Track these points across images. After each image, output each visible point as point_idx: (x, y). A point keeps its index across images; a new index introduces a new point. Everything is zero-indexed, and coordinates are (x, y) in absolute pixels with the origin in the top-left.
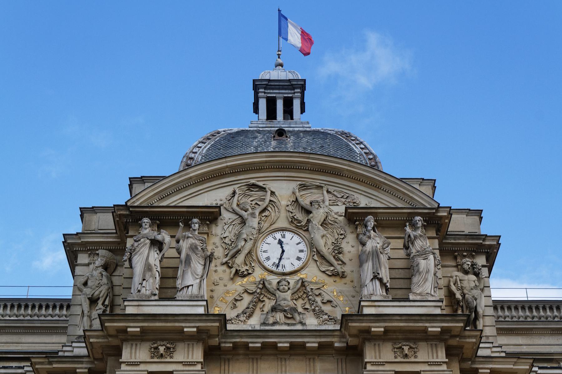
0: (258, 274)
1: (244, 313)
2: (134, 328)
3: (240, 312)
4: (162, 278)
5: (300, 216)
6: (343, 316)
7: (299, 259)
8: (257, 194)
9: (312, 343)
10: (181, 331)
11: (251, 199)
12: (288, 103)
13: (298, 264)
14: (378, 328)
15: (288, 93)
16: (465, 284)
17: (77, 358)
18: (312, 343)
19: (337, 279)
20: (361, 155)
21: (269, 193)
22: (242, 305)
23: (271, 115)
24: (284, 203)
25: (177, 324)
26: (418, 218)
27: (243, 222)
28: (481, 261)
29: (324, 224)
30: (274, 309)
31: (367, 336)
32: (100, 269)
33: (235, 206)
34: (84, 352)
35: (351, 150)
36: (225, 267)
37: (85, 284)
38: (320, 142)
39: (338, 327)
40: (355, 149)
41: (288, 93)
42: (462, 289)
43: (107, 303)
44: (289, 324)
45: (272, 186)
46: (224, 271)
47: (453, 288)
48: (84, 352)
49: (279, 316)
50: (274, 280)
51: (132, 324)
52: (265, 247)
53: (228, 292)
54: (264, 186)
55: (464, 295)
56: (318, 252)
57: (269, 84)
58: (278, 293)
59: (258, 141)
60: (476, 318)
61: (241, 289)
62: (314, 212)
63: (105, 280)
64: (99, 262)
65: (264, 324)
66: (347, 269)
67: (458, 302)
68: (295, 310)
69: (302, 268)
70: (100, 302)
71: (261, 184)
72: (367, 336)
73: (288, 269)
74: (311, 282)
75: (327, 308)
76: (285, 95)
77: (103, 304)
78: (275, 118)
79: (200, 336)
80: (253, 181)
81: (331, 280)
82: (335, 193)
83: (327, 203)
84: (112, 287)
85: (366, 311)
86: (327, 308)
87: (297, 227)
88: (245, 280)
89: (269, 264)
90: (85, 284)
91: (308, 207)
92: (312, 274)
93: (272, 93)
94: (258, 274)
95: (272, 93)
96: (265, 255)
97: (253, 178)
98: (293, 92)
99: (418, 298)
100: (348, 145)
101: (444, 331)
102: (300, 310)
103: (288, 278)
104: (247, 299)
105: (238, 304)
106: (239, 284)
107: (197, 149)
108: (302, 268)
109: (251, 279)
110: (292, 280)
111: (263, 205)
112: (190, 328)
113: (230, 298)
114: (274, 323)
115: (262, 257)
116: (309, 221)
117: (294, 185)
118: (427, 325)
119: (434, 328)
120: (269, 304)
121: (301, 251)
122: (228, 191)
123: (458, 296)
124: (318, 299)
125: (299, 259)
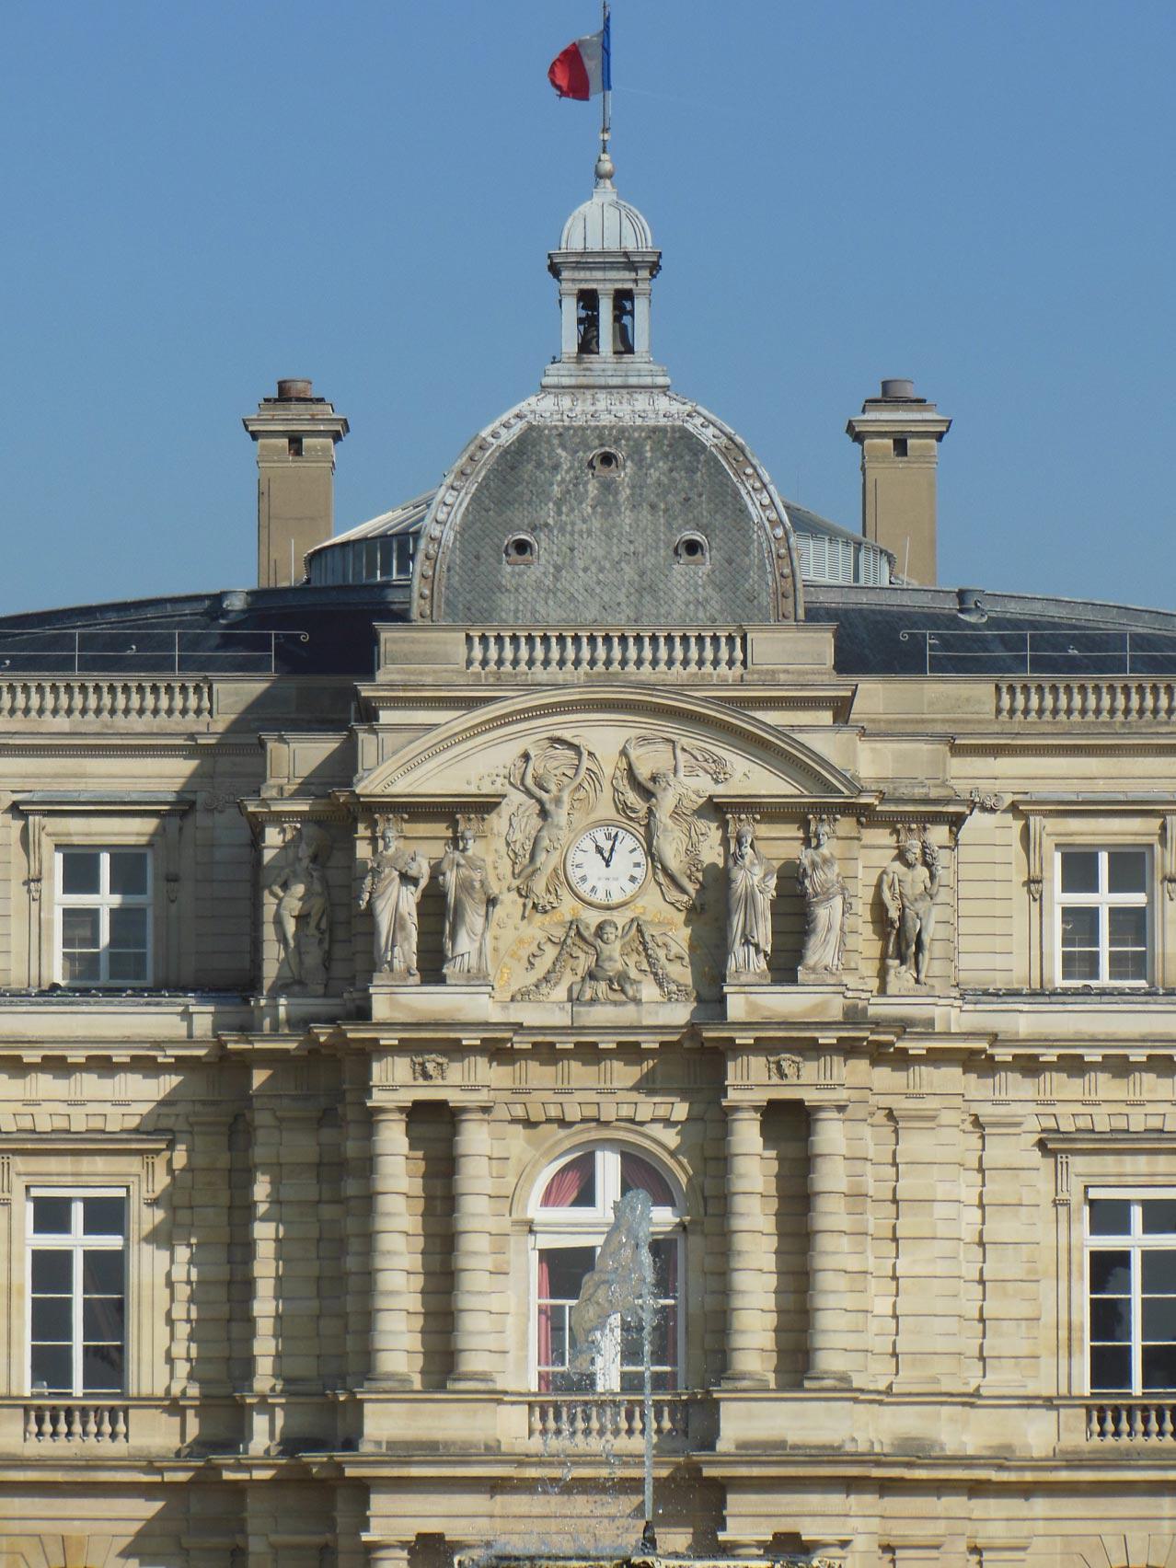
0: (568, 907)
1: (546, 979)
3: (541, 975)
7: (633, 879)
11: (556, 764)
12: (623, 299)
13: (631, 889)
15: (622, 279)
16: (908, 891)
20: (762, 527)
22: (544, 964)
25: (452, 1035)
30: (591, 976)
33: (529, 781)
35: (743, 510)
36: (514, 895)
40: (751, 509)
41: (622, 279)
43: (323, 925)
44: (615, 1003)
46: (514, 902)
50: (592, 918)
51: (386, 1035)
53: (521, 941)
54: (576, 741)
56: (665, 870)
57: (584, 261)
59: (563, 480)
61: (541, 936)
65: (574, 1000)
68: (623, 978)
70: (313, 923)
71: (567, 735)
73: (616, 898)
74: (651, 922)
76: (619, 286)
77: (318, 927)
80: (558, 734)
82: (696, 753)
87: (631, 819)
88: (547, 918)
89: (583, 889)
91: (650, 785)
94: (568, 907)
96: (579, 872)
98: (633, 275)
100: (737, 494)
102: (633, 974)
104: (551, 952)
105: (536, 961)
106: (536, 929)
107: (445, 509)
109: (555, 916)
110: (621, 918)
113: (524, 953)
114: (593, 1001)
115: (574, 875)
116: (650, 812)
118: (817, 1034)
120: (585, 962)
121: (637, 865)
125: (633, 879)
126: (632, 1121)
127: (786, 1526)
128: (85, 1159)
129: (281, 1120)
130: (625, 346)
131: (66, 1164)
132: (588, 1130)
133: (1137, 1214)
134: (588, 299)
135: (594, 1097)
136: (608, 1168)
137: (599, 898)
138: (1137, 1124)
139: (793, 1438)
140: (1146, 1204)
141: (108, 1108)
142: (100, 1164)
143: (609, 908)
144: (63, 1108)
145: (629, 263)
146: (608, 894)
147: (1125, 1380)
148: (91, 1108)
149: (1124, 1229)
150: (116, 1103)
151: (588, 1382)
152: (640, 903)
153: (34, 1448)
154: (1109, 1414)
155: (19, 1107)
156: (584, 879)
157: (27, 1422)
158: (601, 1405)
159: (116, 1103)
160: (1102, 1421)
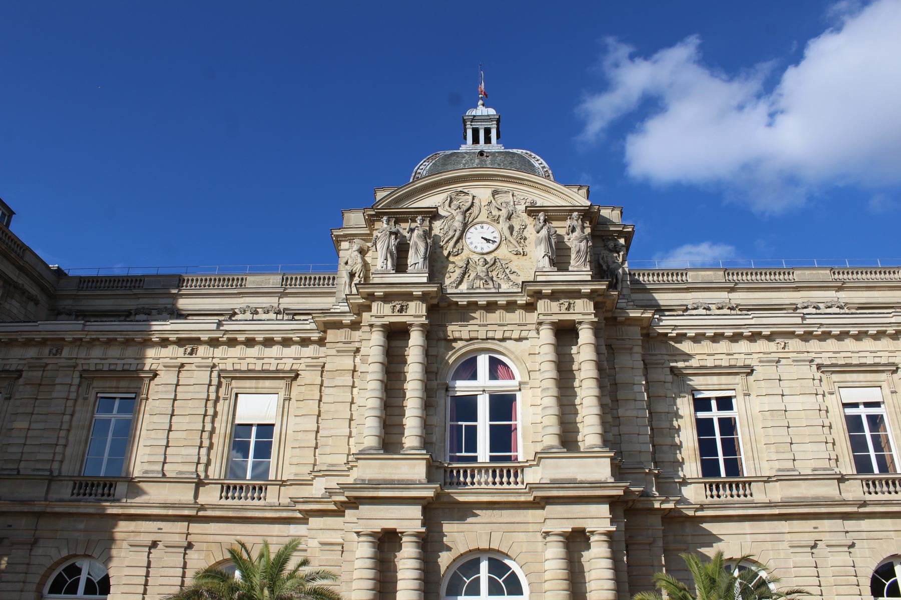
2: (379, 292)
4: (398, 258)
5: (495, 212)
6: (523, 282)
8: (463, 198)
9: (502, 301)
10: (411, 294)
12: (488, 131)
14: (547, 290)
15: (487, 125)
17: (342, 313)
18: (502, 301)
19: (520, 256)
21: (470, 198)
23: (476, 140)
24: (483, 204)
26: (576, 214)
27: (453, 218)
28: (622, 241)
29: (509, 218)
31: (538, 295)
32: (356, 253)
34: (347, 309)
37: (346, 263)
38: (509, 159)
39: (520, 290)
41: (487, 125)
42: (607, 262)
45: (473, 192)
47: (601, 262)
48: (347, 309)
49: (478, 283)
50: (475, 257)
52: (469, 235)
55: (608, 266)
57: (474, 119)
58: (479, 268)
60: (617, 282)
62: (503, 210)
63: (360, 260)
64: (355, 247)
65: (468, 289)
66: (526, 250)
67: (605, 271)
69: (495, 250)
70: (357, 275)
71: (466, 191)
72: (538, 295)
73: (485, 251)
75: (512, 277)
78: (478, 143)
79: (424, 298)
81: (516, 257)
83: (512, 203)
84: (366, 265)
85: (539, 279)
86: (512, 277)
89: (472, 247)
90: (346, 263)
92: (503, 253)
93: (476, 125)
95: (476, 125)
97: (459, 187)
99: (575, 269)
101: (593, 291)
103: (485, 256)
108: (495, 250)
111: (469, 204)
112: (417, 292)
117: (489, 192)
119: (586, 289)
120: (473, 275)
122: (444, 195)
123: (605, 267)
124: (507, 271)
126: (493, 339)
127: (578, 524)
128: (261, 381)
129: (338, 351)
130: (488, 140)
131: (252, 383)
132: (473, 344)
133: (714, 403)
134: (476, 132)
135: (476, 328)
136: (483, 363)
137: (479, 250)
138: (710, 362)
139: (580, 477)
140: (717, 399)
141: (272, 361)
142: (267, 383)
143: (483, 254)
144: (254, 361)
145: (488, 119)
146: (482, 249)
147: (718, 474)
148: (265, 361)
149: (710, 409)
150: (276, 359)
151: (474, 459)
152: (496, 252)
153: (223, 502)
154: (714, 486)
155: (236, 360)
156: (471, 243)
157: (222, 492)
158: (480, 469)
159: (276, 359)
160: (711, 490)
